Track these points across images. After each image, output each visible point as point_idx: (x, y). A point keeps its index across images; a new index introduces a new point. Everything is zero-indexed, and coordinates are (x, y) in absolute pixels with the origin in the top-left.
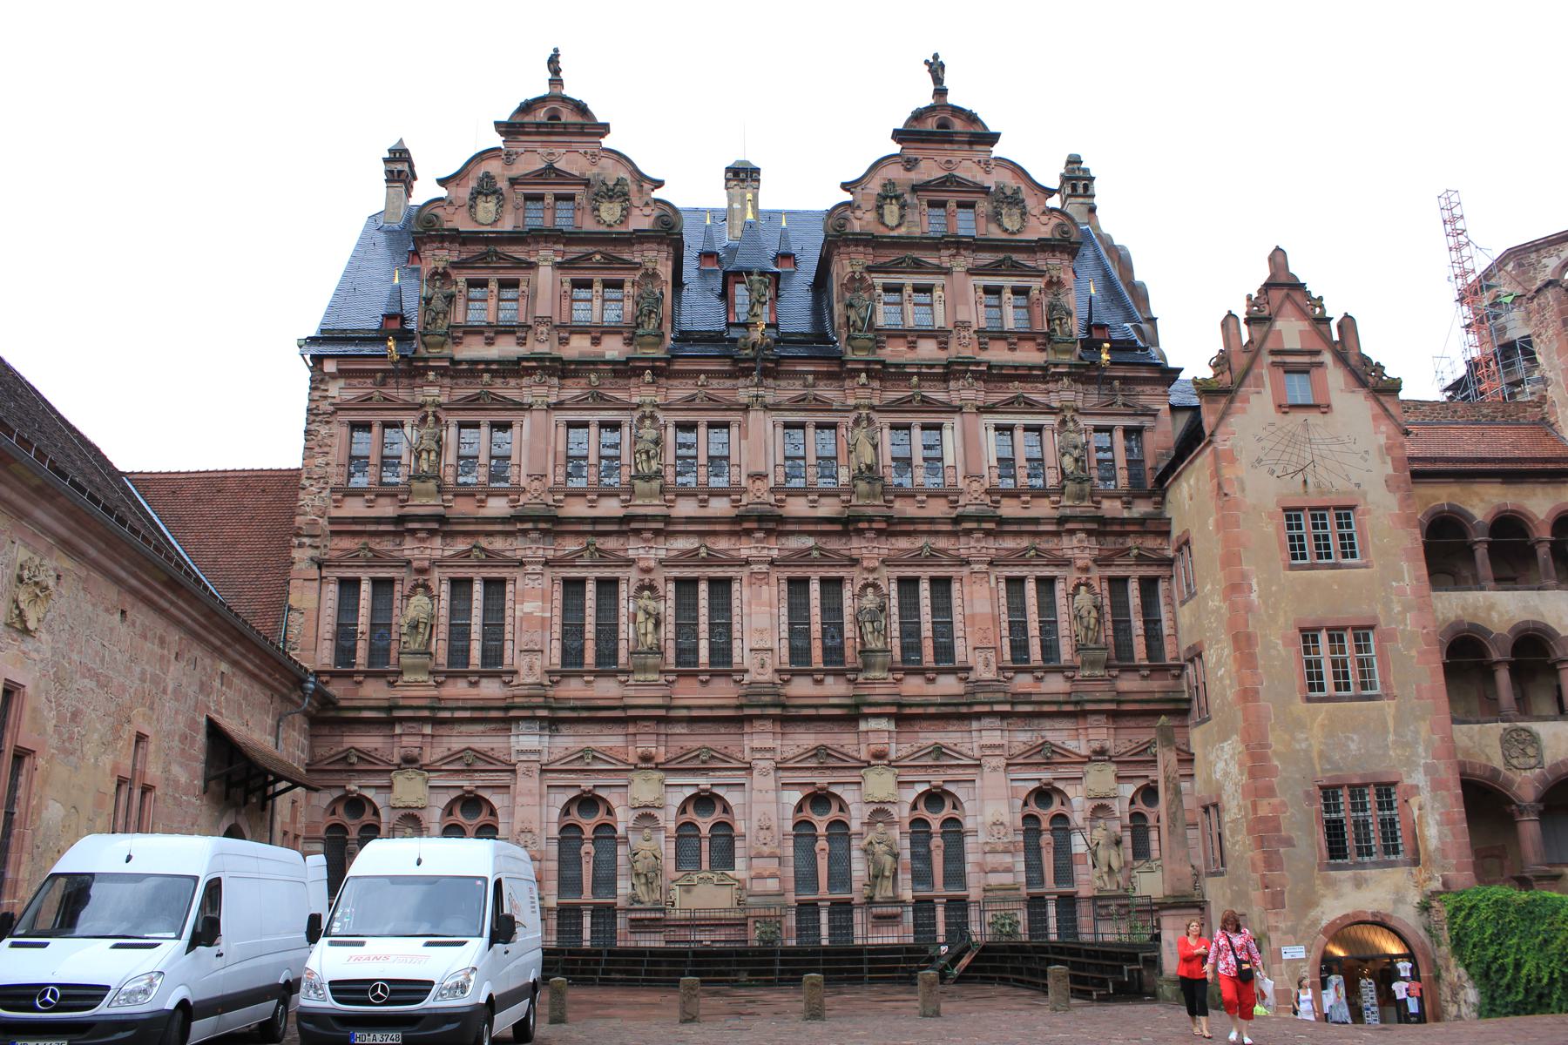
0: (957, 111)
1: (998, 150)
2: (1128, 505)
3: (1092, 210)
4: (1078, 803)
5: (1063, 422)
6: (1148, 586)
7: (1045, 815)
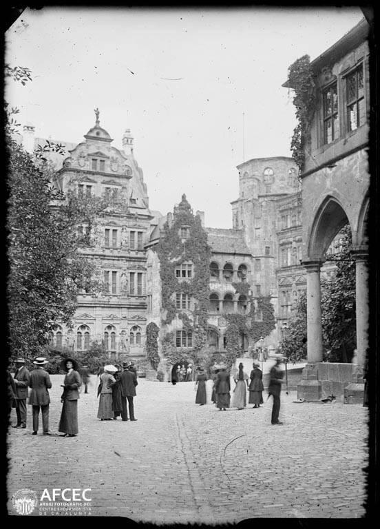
0: (103, 130)
1: (112, 144)
2: (137, 254)
3: (132, 150)
4: (118, 331)
5: (123, 229)
6: (140, 274)
7: (110, 332)
